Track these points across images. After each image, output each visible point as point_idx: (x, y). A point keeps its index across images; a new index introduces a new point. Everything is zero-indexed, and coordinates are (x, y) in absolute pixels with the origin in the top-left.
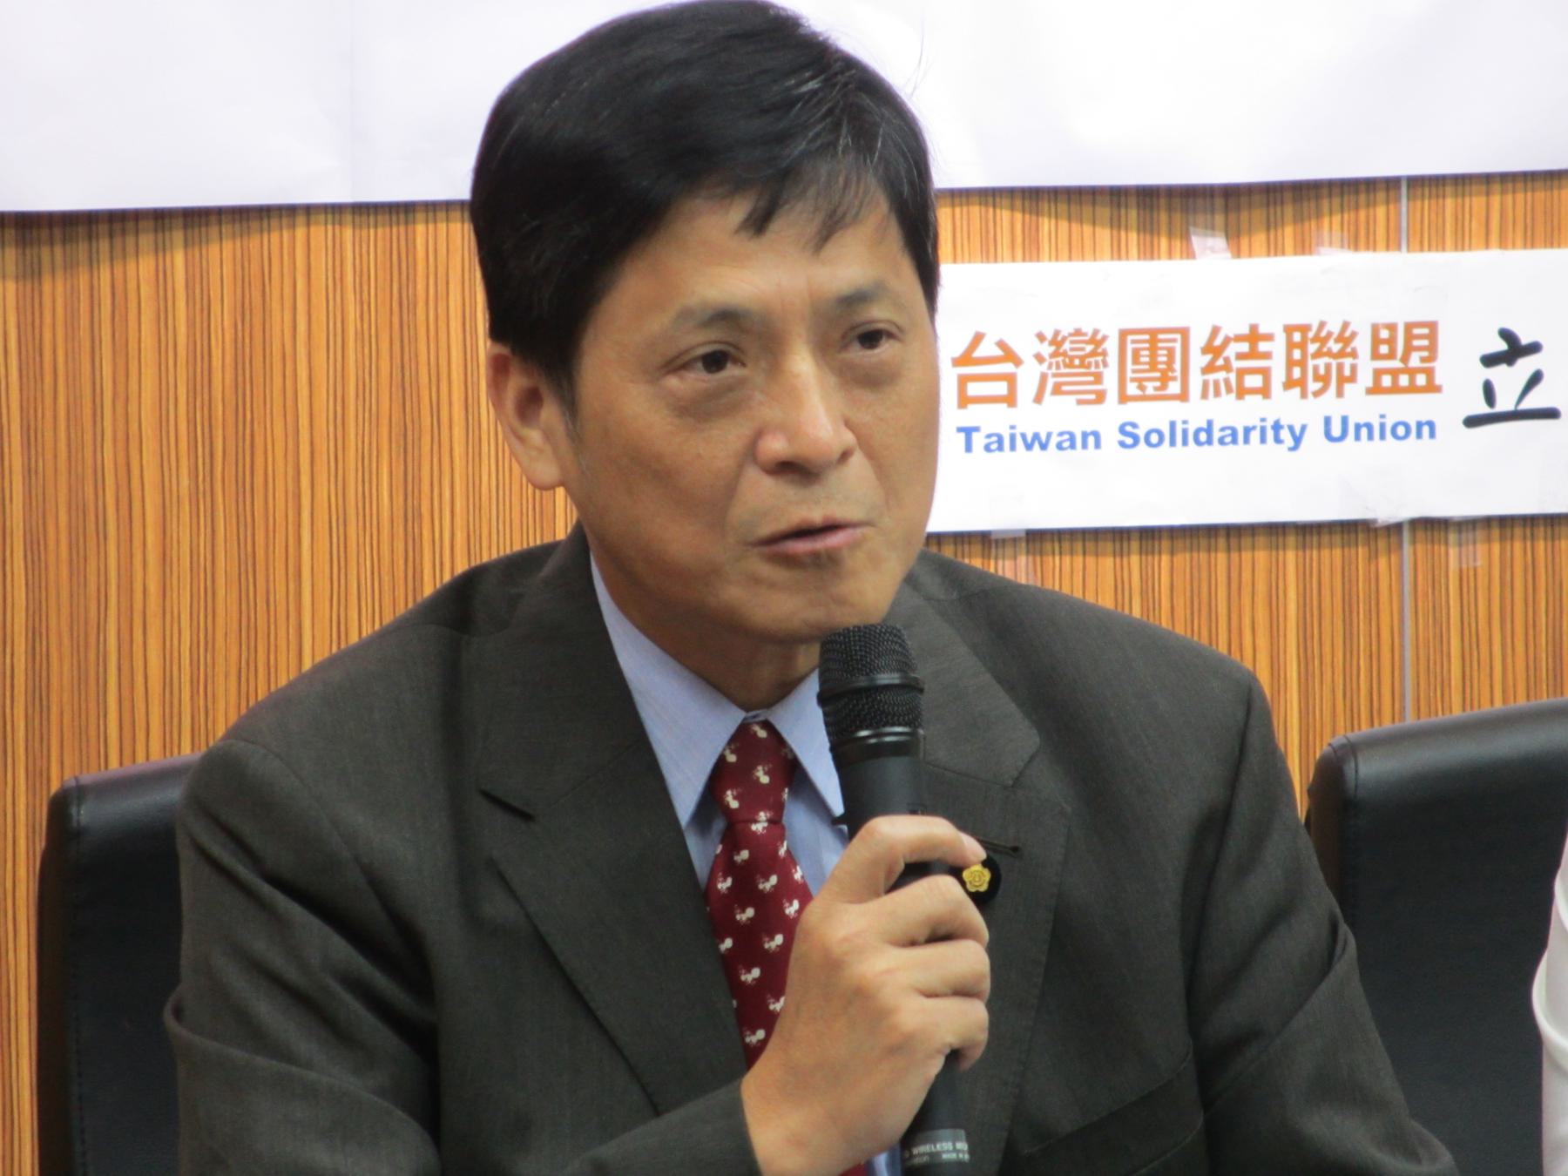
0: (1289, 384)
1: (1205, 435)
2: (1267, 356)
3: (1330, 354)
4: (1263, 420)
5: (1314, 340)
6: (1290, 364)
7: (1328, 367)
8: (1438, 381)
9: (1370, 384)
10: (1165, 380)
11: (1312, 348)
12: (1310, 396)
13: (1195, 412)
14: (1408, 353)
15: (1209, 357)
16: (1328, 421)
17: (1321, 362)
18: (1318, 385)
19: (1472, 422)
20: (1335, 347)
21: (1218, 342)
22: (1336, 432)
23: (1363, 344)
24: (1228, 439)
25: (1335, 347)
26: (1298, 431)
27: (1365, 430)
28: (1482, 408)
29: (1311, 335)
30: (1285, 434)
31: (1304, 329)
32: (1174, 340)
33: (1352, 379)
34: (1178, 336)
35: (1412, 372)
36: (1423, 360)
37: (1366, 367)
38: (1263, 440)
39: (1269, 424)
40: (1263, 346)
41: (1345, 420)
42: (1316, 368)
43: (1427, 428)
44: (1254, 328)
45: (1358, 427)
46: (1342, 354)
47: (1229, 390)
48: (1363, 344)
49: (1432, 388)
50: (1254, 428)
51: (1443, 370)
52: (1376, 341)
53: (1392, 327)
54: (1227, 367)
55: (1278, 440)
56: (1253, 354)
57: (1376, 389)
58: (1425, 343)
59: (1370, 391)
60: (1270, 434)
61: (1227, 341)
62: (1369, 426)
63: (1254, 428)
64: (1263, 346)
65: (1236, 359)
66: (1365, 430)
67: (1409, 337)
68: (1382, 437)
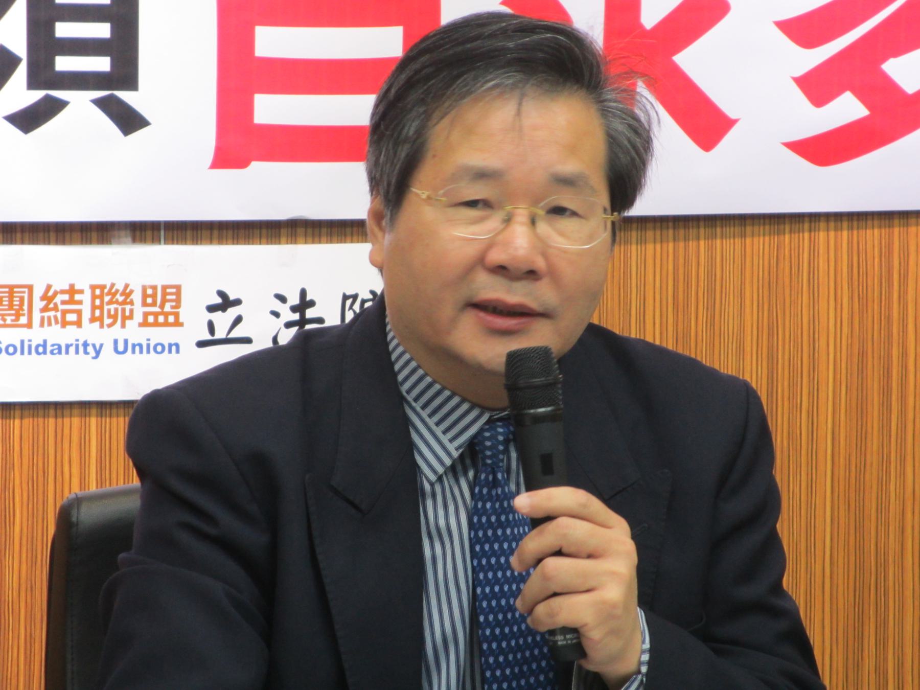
0: (93, 319)
1: (42, 348)
2: (80, 302)
3: (117, 302)
4: (77, 340)
5: (108, 294)
6: (94, 307)
7: (116, 310)
8: (181, 321)
9: (141, 321)
10: (18, 316)
11: (107, 299)
12: (105, 327)
13: (36, 335)
15: (44, 303)
16: (116, 342)
17: (112, 307)
18: (110, 321)
19: (202, 344)
20: (121, 299)
21: (50, 294)
22: (121, 348)
23: (137, 297)
24: (56, 351)
25: (121, 299)
26: (98, 348)
27: (138, 348)
28: (207, 337)
29: (106, 291)
30: (90, 349)
31: (102, 287)
32: (24, 292)
33: (131, 317)
34: (26, 290)
35: (166, 315)
36: (172, 307)
37: (139, 311)
38: (77, 352)
39: (81, 343)
40: (77, 297)
41: (126, 341)
42: (109, 311)
44: (72, 286)
45: (134, 346)
46: (124, 303)
47: (57, 322)
48: (137, 297)
49: (178, 323)
50: (71, 345)
51: (184, 314)
52: (145, 296)
53: (154, 288)
54: (56, 308)
55: (86, 353)
56: (72, 301)
57: (144, 324)
58: (174, 297)
59: (141, 325)
60: (81, 349)
61: (56, 293)
62: (140, 346)
63: (71, 345)
64: (77, 297)
65: (60, 304)
66: (138, 348)
68: (148, 352)
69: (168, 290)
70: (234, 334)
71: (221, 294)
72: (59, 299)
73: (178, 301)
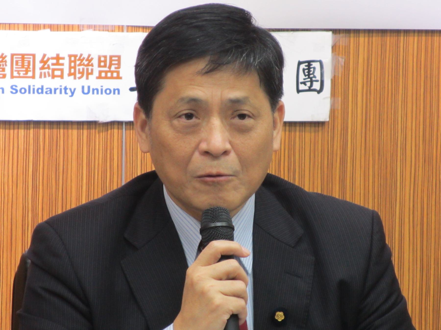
0: (70, 74)
2: (62, 64)
4: (61, 86)
7: (83, 69)
12: (77, 78)
33: (92, 73)
36: (116, 68)
40: (61, 61)
43: (117, 91)
46: (88, 65)
59: (97, 78)
64: (61, 61)
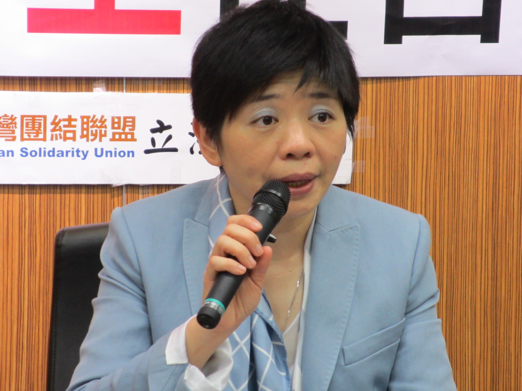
0: (82, 136)
1: (52, 153)
2: (75, 126)
3: (97, 126)
4: (73, 149)
5: (91, 122)
6: (83, 129)
7: (96, 131)
8: (135, 137)
9: (111, 137)
10: (37, 134)
11: (91, 124)
12: (90, 141)
13: (48, 145)
14: (125, 127)
15: (53, 126)
16: (96, 150)
17: (94, 129)
18: (93, 137)
19: (147, 152)
20: (99, 124)
21: (57, 121)
22: (99, 153)
23: (109, 123)
24: (60, 155)
25: (99, 124)
27: (109, 153)
28: (151, 147)
29: (90, 120)
30: (81, 154)
32: (41, 120)
33: (105, 135)
34: (42, 118)
35: (126, 134)
36: (130, 130)
37: (110, 132)
38: (73, 156)
39: (75, 150)
40: (73, 123)
41: (102, 150)
42: (92, 131)
44: (70, 116)
45: (107, 152)
46: (101, 127)
48: (109, 123)
49: (133, 139)
50: (70, 151)
51: (137, 134)
52: (113, 123)
53: (119, 118)
54: (60, 129)
55: (78, 156)
56: (70, 125)
57: (113, 139)
58: (131, 124)
59: (111, 140)
60: (75, 154)
61: (60, 121)
62: (111, 152)
63: (70, 151)
64: (73, 123)
65: (63, 127)
66: (109, 153)
67: (125, 122)
68: (115, 156)
69: (128, 120)
70: (167, 146)
71: (159, 122)
72: (62, 124)
73: (133, 126)
